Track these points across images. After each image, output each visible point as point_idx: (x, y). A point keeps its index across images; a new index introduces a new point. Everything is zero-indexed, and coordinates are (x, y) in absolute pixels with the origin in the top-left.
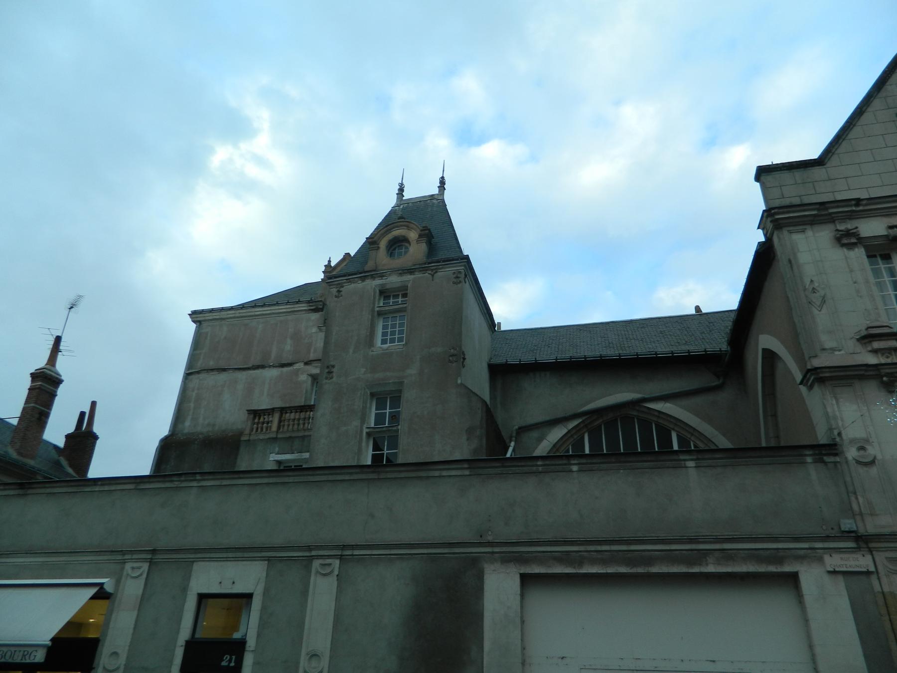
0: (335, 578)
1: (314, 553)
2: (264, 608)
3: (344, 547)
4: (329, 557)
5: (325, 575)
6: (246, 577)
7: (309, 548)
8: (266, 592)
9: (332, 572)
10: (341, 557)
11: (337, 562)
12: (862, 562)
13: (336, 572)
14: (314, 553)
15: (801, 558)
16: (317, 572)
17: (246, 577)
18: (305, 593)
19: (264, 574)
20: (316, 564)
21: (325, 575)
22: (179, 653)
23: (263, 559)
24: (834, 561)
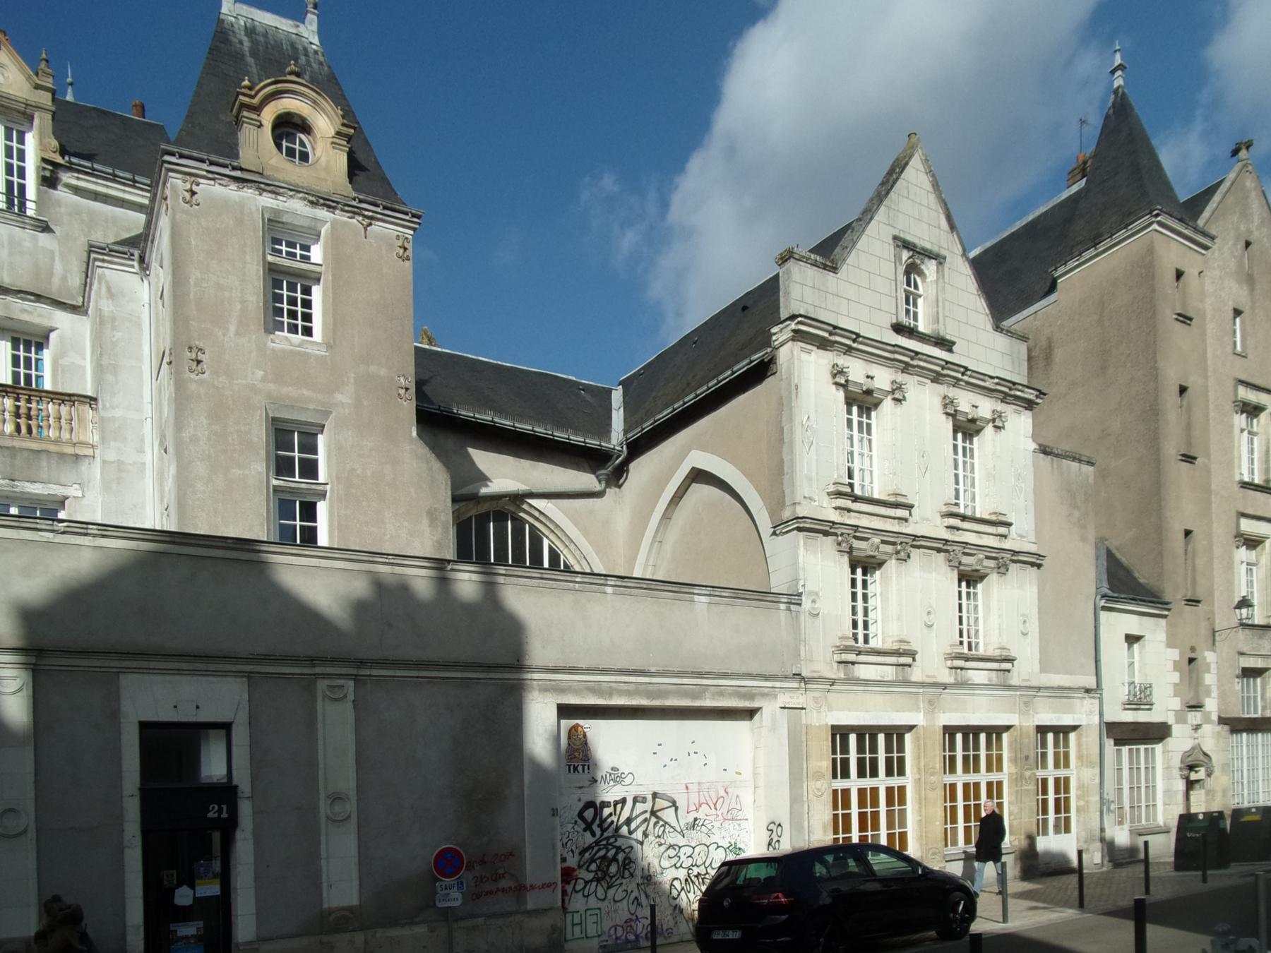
0: (350, 705)
1: (318, 670)
2: (253, 744)
3: (362, 663)
4: (340, 676)
5: (336, 700)
6: (217, 697)
7: (312, 661)
8: (253, 721)
9: (345, 696)
10: (356, 678)
11: (351, 683)
12: (798, 699)
13: (351, 697)
14: (318, 670)
15: (764, 695)
16: (324, 697)
17: (217, 697)
18: (311, 722)
19: (246, 696)
20: (322, 685)
21: (336, 700)
22: (132, 809)
23: (239, 674)
24: (783, 699)
